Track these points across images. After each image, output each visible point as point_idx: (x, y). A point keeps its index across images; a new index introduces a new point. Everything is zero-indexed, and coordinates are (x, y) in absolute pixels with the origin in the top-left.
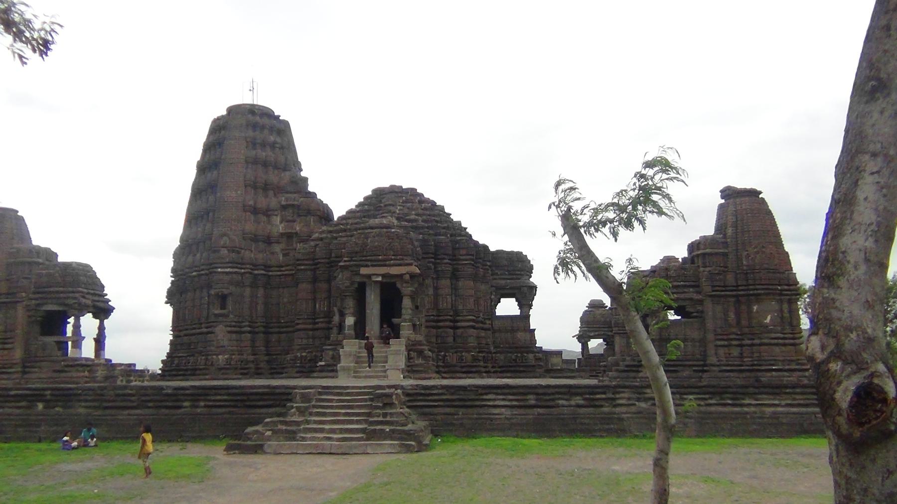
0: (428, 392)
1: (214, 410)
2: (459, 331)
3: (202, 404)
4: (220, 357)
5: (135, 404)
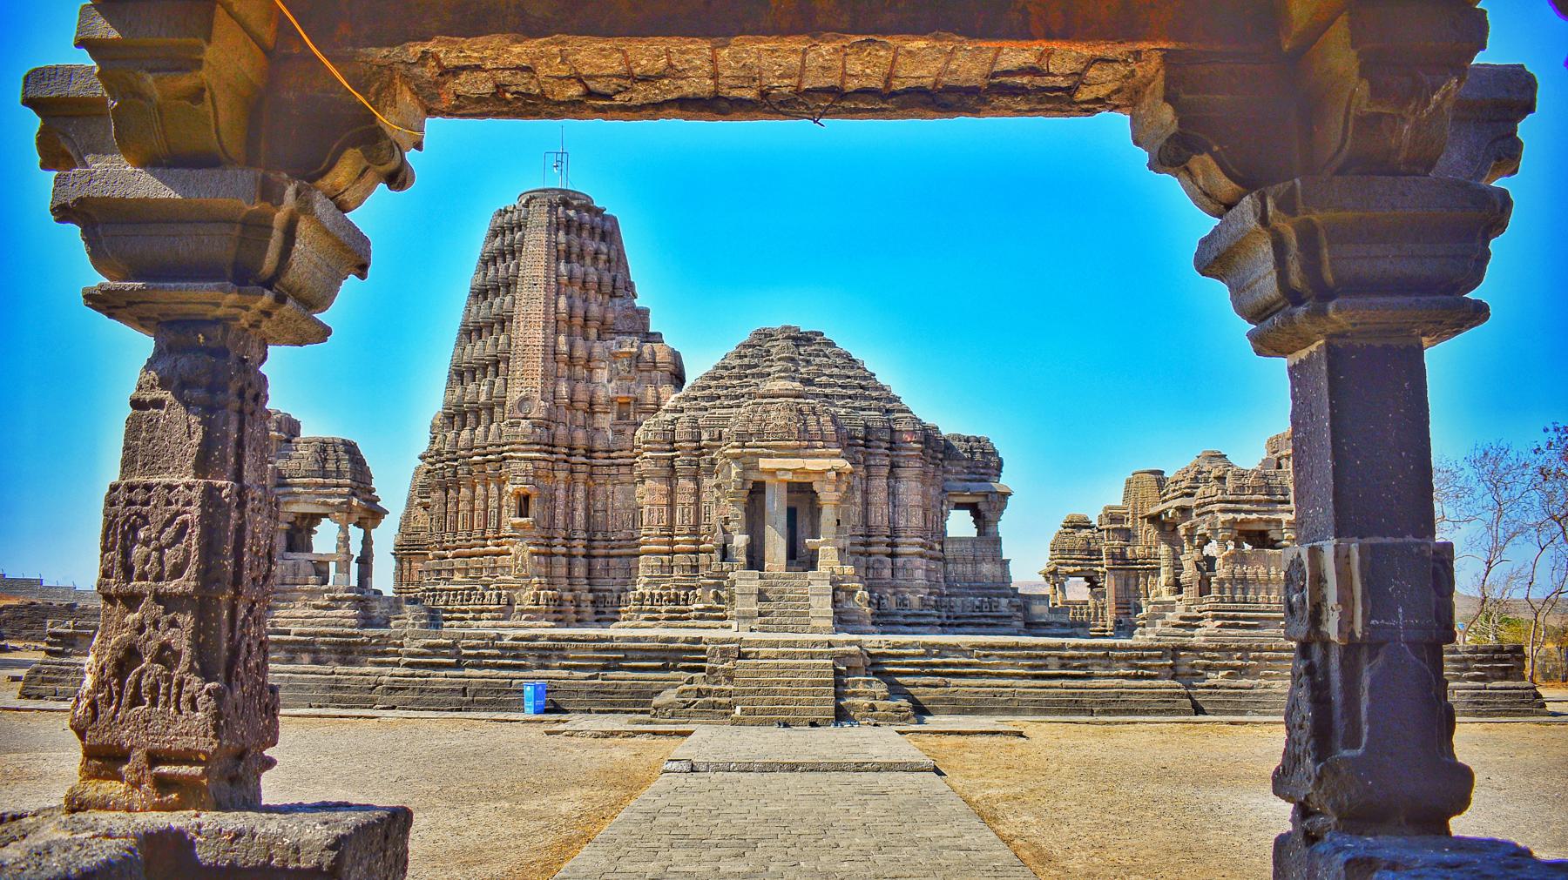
1: (577, 674)
2: (900, 561)
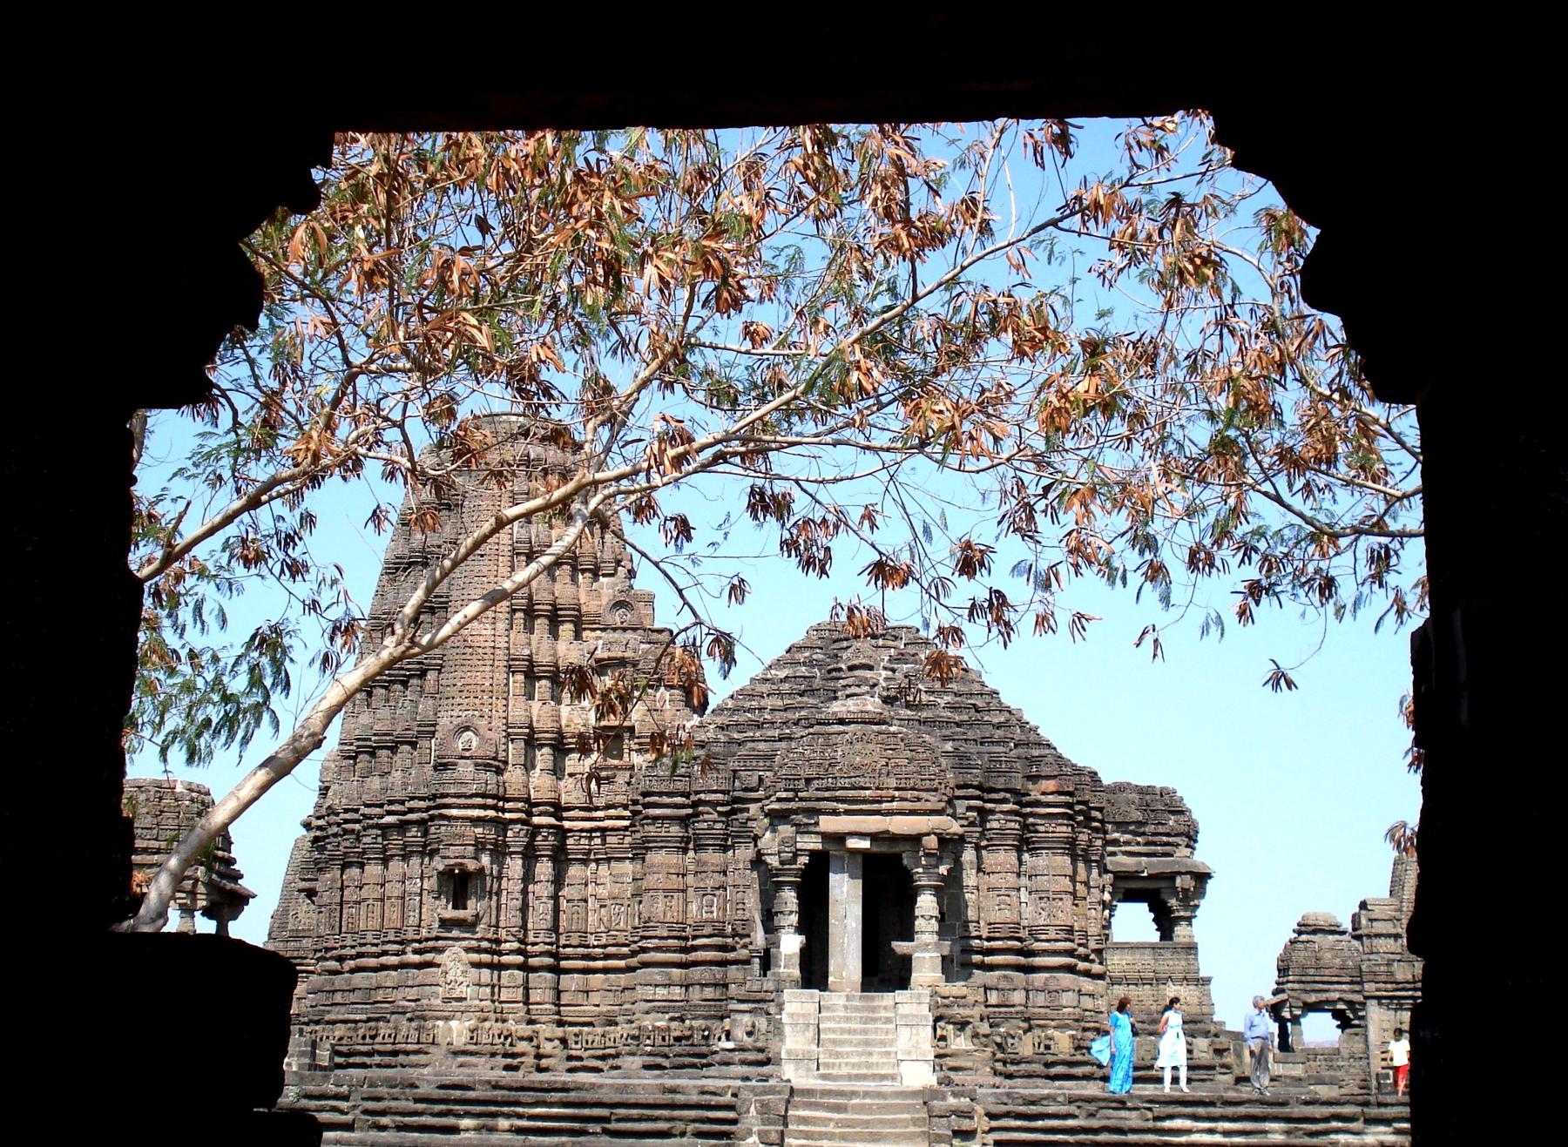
0: (1034, 1109)
3: (504, 1123)
4: (454, 1024)
5: (349, 1117)
